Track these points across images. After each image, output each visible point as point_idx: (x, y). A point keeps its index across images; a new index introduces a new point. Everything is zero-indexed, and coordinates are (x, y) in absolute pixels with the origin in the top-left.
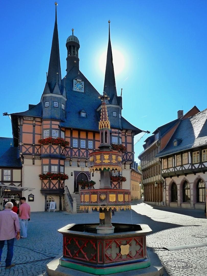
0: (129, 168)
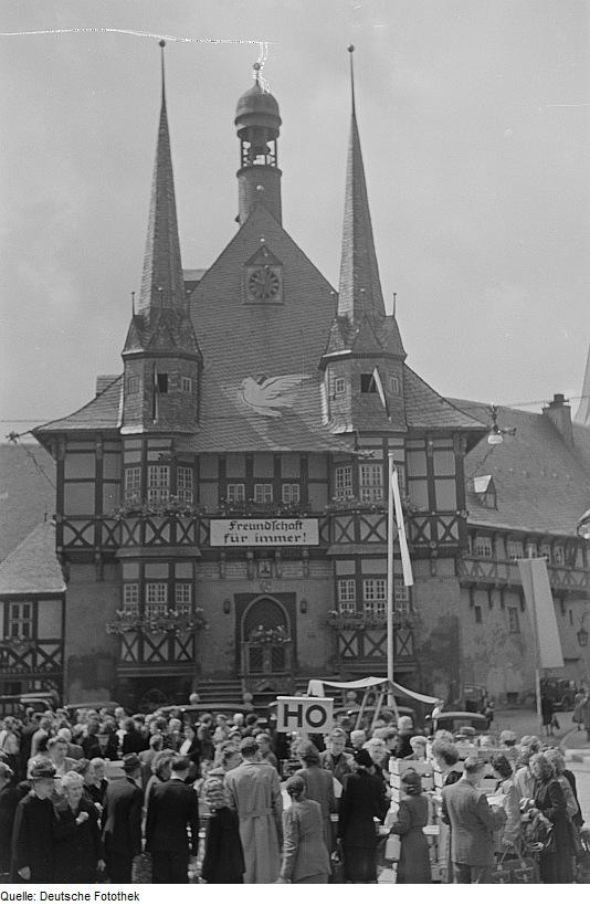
0: (451, 572)
